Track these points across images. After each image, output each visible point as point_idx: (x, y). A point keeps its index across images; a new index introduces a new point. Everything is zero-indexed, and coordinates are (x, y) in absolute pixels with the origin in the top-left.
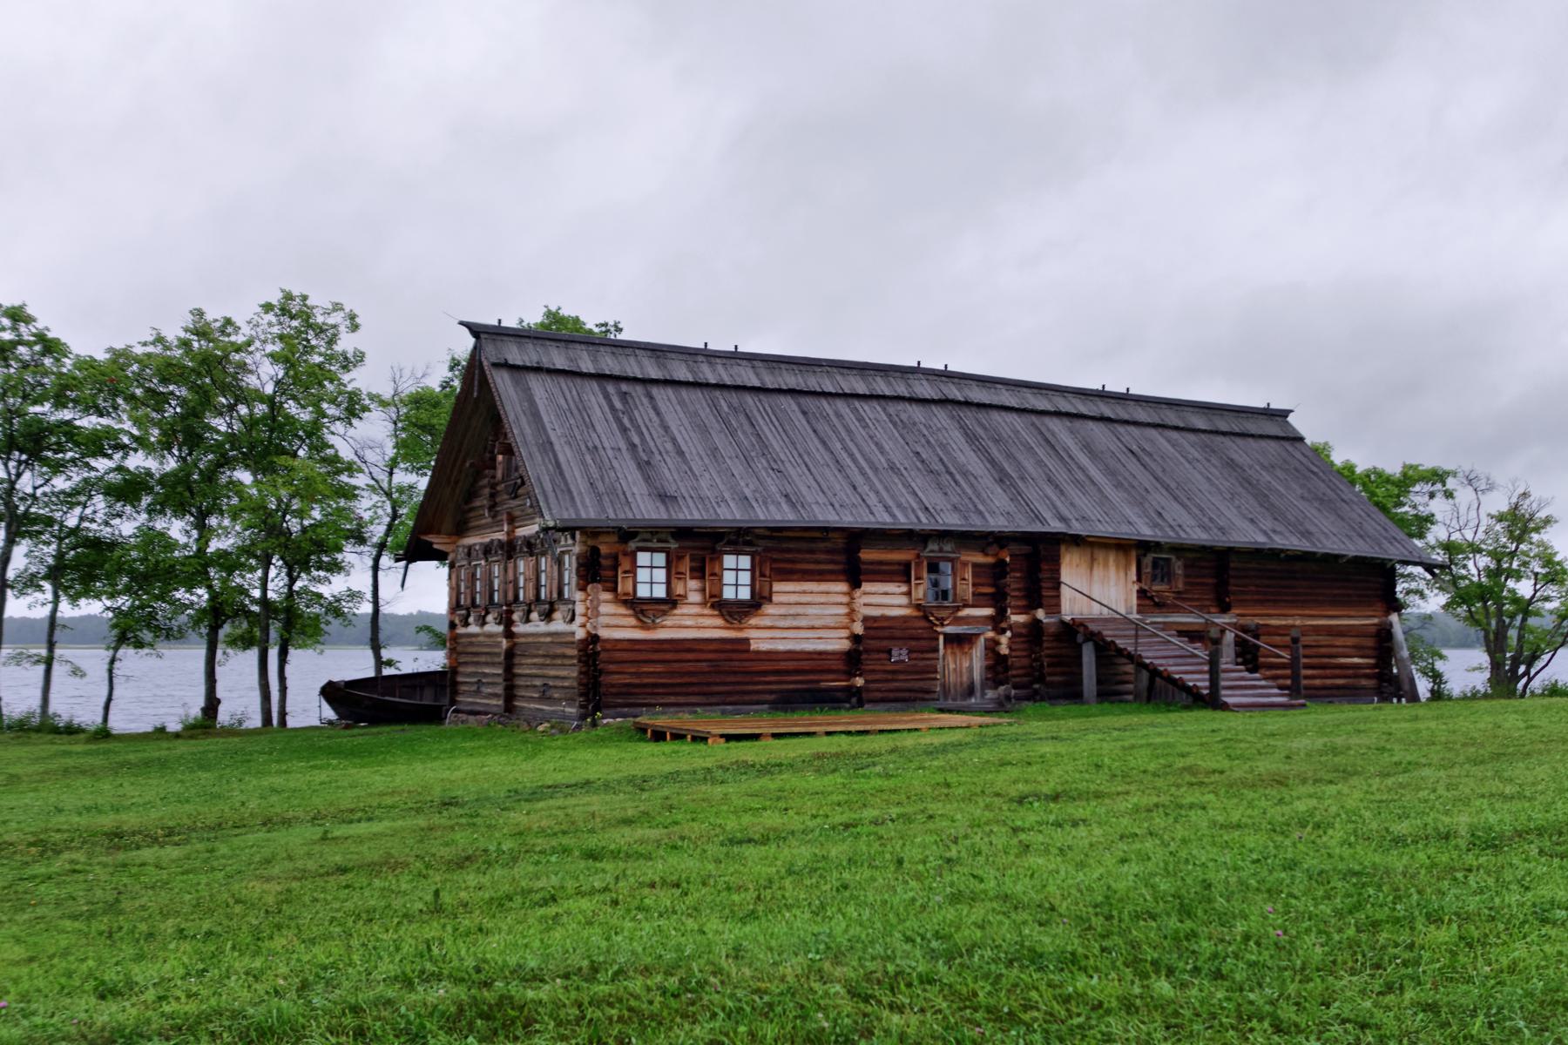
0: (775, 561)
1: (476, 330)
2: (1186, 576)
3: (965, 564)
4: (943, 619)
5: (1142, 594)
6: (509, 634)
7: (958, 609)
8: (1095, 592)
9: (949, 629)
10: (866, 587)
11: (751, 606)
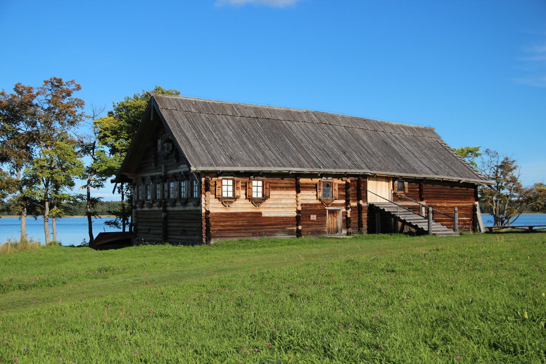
0: (271, 183)
2: (409, 188)
3: (335, 184)
4: (328, 204)
5: (394, 194)
6: (165, 211)
7: (333, 201)
8: (379, 193)
11: (263, 200)
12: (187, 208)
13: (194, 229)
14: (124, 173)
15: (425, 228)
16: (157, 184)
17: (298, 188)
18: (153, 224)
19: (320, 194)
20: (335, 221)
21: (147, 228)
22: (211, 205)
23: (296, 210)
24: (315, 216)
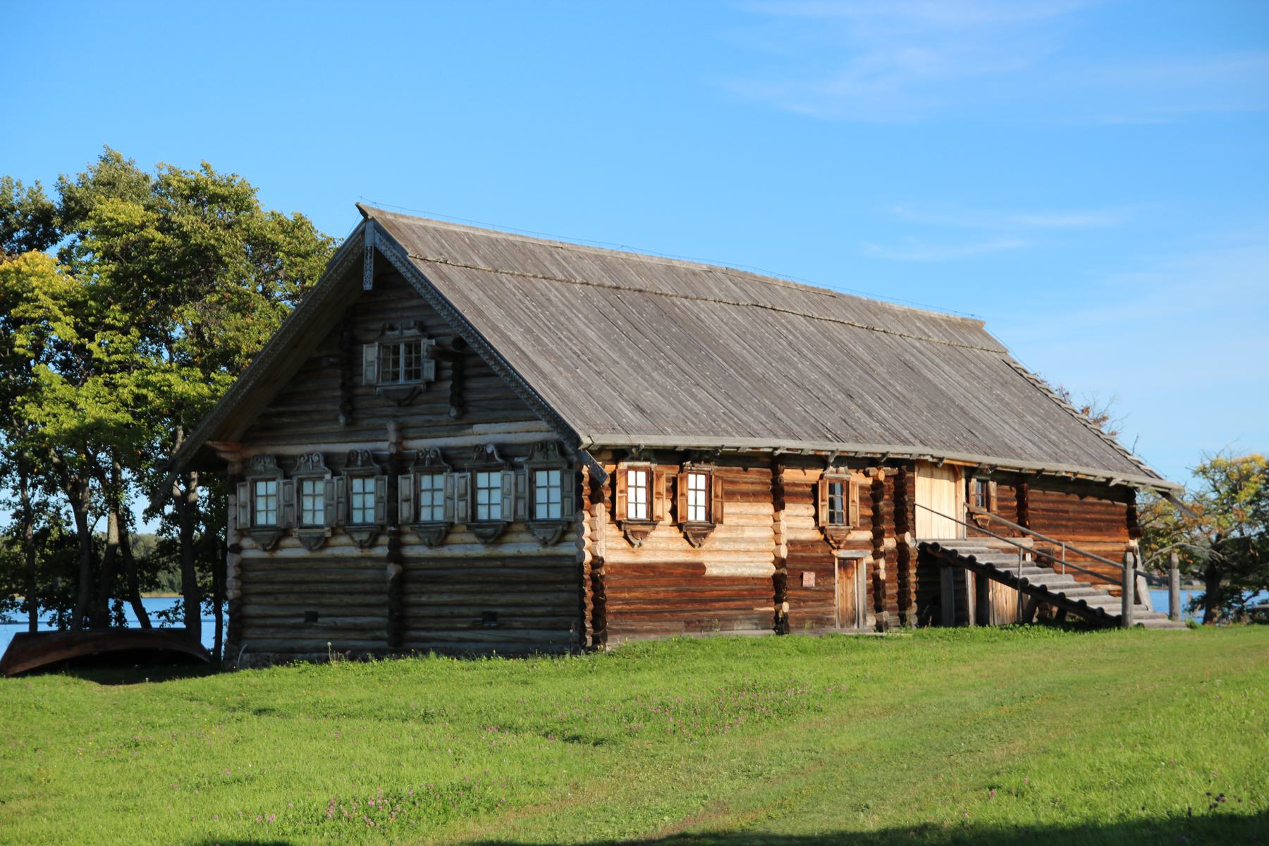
2: (999, 499)
4: (839, 542)
6: (396, 555)
8: (939, 512)
9: (843, 553)
12: (507, 550)
13: (538, 610)
14: (210, 443)
15: (1113, 609)
16: (352, 477)
17: (779, 496)
18: (326, 600)
19: (824, 514)
20: (849, 591)
21: (302, 611)
22: (603, 542)
23: (772, 558)
24: (812, 575)
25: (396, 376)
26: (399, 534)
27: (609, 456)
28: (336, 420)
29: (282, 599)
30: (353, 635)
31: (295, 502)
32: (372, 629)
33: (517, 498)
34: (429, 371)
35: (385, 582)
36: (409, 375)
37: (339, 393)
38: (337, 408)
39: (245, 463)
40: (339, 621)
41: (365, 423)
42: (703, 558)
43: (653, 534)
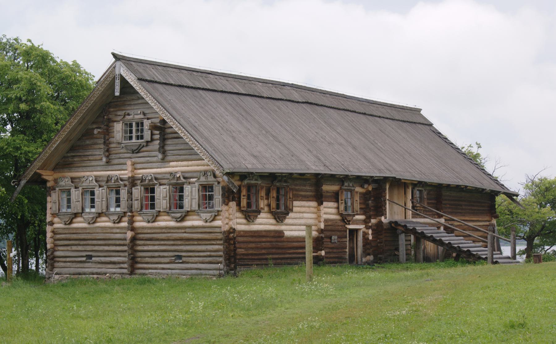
1: (114, 55)
3: (357, 192)
4: (349, 221)
7: (354, 215)
10: (325, 203)
13: (202, 254)
14: (38, 171)
17: (320, 198)
19: (342, 207)
21: (84, 254)
24: (336, 237)
25: (131, 138)
26: (133, 216)
27: (238, 178)
28: (101, 159)
29: (74, 248)
30: (110, 266)
31: (80, 200)
32: (119, 263)
33: (192, 199)
34: (147, 135)
35: (125, 239)
36: (137, 138)
37: (102, 146)
38: (102, 153)
39: (56, 181)
40: (103, 259)
41: (116, 161)
42: (283, 228)
43: (259, 216)
